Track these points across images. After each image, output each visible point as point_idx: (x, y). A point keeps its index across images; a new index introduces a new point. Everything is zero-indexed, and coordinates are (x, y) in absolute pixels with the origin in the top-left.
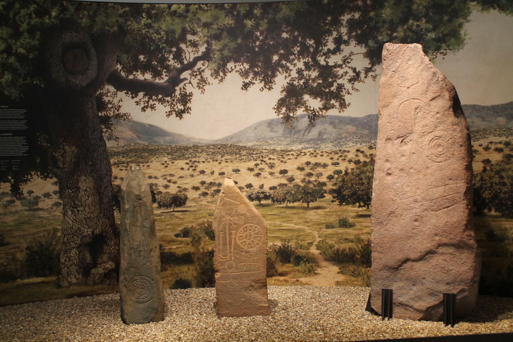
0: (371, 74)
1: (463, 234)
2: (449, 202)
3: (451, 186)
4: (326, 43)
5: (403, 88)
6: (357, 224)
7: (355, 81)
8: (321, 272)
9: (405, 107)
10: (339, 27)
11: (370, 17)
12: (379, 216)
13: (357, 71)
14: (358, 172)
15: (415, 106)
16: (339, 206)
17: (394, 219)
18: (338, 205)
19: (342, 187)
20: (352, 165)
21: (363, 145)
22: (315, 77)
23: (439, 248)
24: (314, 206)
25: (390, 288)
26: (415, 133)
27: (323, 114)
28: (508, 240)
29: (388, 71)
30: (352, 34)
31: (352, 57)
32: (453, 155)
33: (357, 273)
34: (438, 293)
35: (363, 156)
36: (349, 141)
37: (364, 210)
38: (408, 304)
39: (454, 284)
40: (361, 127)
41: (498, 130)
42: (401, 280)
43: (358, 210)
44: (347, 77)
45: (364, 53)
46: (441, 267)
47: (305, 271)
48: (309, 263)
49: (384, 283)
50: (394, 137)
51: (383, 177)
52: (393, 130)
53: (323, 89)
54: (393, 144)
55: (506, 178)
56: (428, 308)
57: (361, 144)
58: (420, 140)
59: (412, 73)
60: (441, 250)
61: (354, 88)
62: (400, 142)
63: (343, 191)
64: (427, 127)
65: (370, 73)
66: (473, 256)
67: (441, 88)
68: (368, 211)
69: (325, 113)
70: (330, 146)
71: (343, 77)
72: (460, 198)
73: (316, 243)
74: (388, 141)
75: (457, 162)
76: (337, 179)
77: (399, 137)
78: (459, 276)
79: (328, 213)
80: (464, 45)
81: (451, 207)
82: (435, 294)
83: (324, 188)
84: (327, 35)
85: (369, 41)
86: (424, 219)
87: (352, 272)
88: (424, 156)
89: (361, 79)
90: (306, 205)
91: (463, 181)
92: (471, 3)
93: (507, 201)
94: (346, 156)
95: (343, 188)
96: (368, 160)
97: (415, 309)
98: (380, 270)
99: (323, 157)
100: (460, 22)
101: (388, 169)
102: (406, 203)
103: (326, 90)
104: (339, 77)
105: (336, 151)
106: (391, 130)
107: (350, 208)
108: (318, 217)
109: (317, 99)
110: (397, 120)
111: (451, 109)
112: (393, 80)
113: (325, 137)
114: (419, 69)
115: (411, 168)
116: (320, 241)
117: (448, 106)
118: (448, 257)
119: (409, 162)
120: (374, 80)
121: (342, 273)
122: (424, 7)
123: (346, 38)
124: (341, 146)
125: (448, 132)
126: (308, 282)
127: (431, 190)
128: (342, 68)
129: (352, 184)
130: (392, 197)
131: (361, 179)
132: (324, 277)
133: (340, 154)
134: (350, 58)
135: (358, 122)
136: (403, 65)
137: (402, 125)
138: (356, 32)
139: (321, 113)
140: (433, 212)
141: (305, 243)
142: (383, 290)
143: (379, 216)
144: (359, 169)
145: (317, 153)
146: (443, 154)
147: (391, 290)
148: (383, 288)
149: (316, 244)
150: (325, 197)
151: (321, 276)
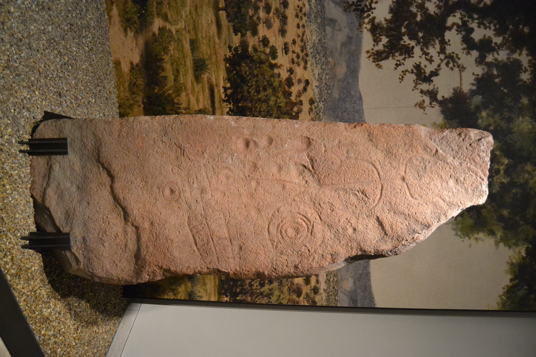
0: (427, 100)
1: (154, 264)
2: (204, 245)
3: (230, 248)
4: (484, 25)
5: (404, 169)
6: (200, 86)
7: (416, 75)
8: (129, 37)
9: (367, 172)
10: (508, 46)
11: (520, 98)
12: (177, 128)
13: (432, 78)
14: (276, 84)
15: (369, 190)
16: (224, 57)
17: (173, 155)
18: (225, 55)
19: (252, 61)
20: (284, 75)
21: (316, 91)
22: (427, 9)
23: (133, 228)
24: (221, 18)
25: (69, 150)
27: (365, 25)
28: (192, 286)
29: (437, 140)
30: (495, 69)
31: (456, 70)
33: (135, 89)
34: (69, 225)
35: (299, 90)
36: (321, 68)
37: (220, 95)
38: (51, 180)
39: (85, 248)
40: (343, 86)
41: (336, 279)
42: (83, 167)
43: (220, 87)
44: (424, 62)
45: (461, 89)
46: (107, 230)
47: (127, 13)
48: (139, 18)
49: (76, 140)
50: (313, 152)
52: (325, 151)
53: (406, 23)
55: (270, 287)
56: (48, 209)
57: (316, 86)
58: (306, 198)
60: (130, 230)
61: (405, 74)
62: (304, 163)
63: (246, 63)
64: (329, 210)
65: (428, 98)
66: (126, 277)
67: (399, 236)
68: (220, 102)
69: (366, 28)
70: (314, 38)
71: (424, 56)
72: (210, 263)
73: (168, 26)
75: (269, 260)
76: (264, 52)
77: (312, 161)
78: (96, 257)
79: (212, 43)
80: (461, 238)
81: (195, 248)
82: (68, 221)
83: (249, 34)
84: (497, 26)
85: (480, 97)
86: (174, 204)
87: (135, 83)
89: (420, 84)
90: (221, 6)
91: (238, 268)
92: (524, 249)
93: (241, 288)
94: (299, 65)
95: (250, 63)
96: (293, 98)
97: (45, 189)
98: (94, 134)
99: (295, 29)
100: (496, 232)
101: (256, 144)
102: (199, 175)
103: (405, 28)
104: (425, 49)
105: (306, 49)
106: (325, 146)
107: (222, 74)
108: (205, 25)
109: (389, 13)
110: (343, 158)
111: (360, 253)
112: (420, 151)
113: (328, 29)
114: (437, 198)
115: (258, 183)
116: (172, 33)
117: (367, 248)
118: (121, 240)
119: (268, 180)
120: (416, 105)
121: (132, 68)
122: (527, 182)
123: (490, 58)
124: (314, 57)
126: (112, 19)
127: (222, 215)
128: (439, 53)
129: (257, 76)
130: (208, 151)
131: (265, 89)
132: (123, 43)
133: (301, 55)
134: (454, 66)
135: (350, 81)
136: (448, 169)
137: (335, 167)
138: (498, 76)
139: (366, 20)
140: (186, 219)
141: (165, 9)
142: (66, 139)
143: (177, 128)
144: (280, 86)
145: (301, 18)
146: (283, 237)
147: (66, 153)
148: (69, 140)
149: (166, 27)
150: (236, 35)
151: (123, 37)
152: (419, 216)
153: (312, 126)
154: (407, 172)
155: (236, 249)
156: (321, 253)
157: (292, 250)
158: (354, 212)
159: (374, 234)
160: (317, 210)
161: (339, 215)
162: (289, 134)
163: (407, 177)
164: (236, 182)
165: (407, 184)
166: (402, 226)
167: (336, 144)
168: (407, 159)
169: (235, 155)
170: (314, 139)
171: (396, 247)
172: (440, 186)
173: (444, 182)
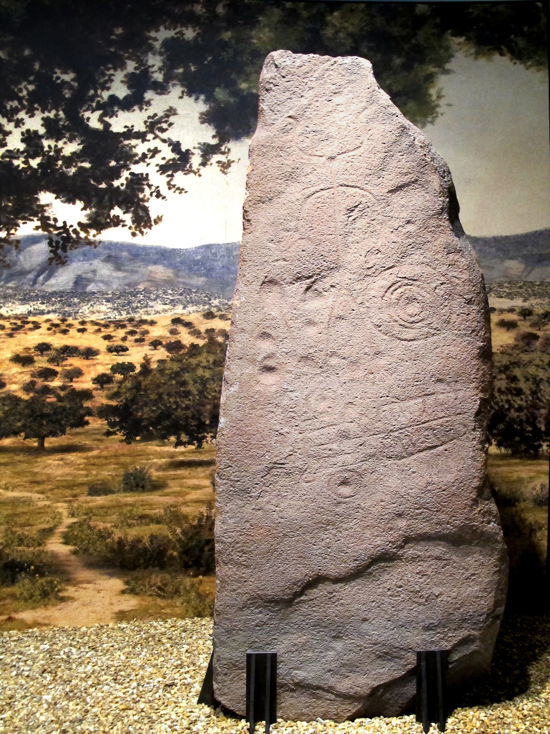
9: (319, 205)
50: (285, 276)
58: (359, 287)
67: (419, 165)
88: (370, 326)
110: (297, 236)
111: (445, 216)
117: (438, 207)
137: (310, 247)
152: (388, 139)
153: (244, 279)
158: (381, 223)
163: (329, 154)
166: (404, 161)
167: (274, 246)
170: (265, 275)
171: (436, 169)
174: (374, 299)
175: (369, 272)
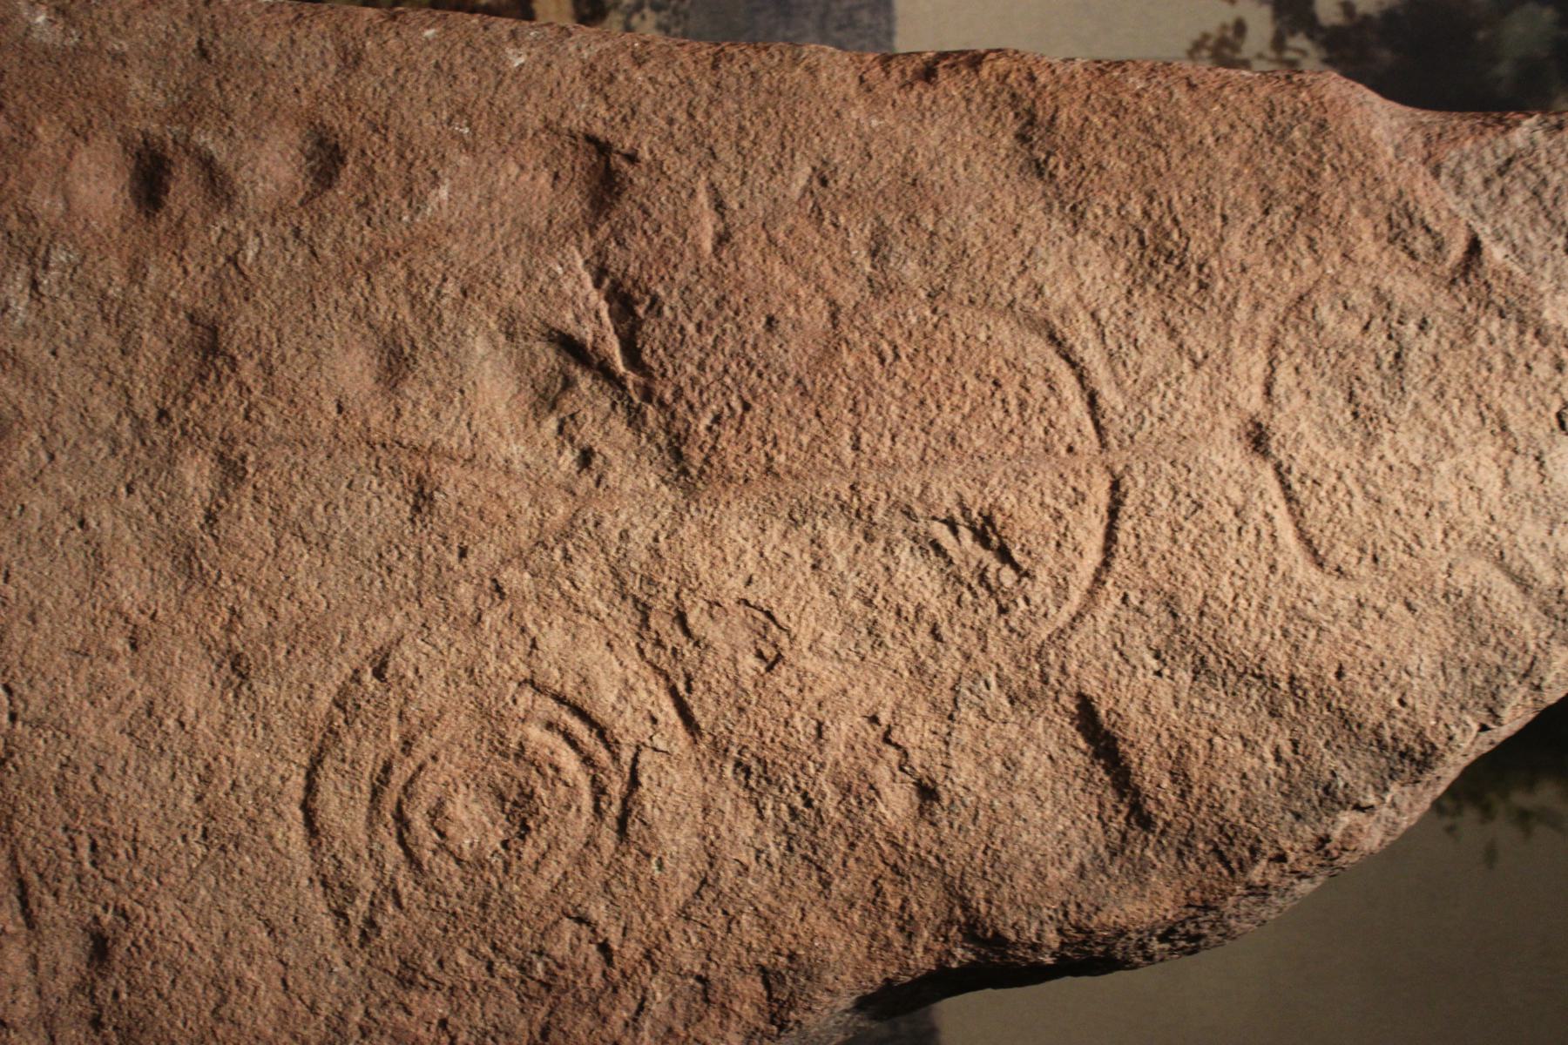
5: (1259, 371)
9: (1011, 390)
26: (678, 515)
29: (1475, 180)
32: (408, 976)
50: (638, 243)
51: (116, 100)
52: (722, 239)
54: (538, 240)
58: (584, 574)
59: (1444, 489)
64: (749, 662)
65: (1266, 11)
74: (576, 163)
85: (1548, 14)
88: (381, 629)
106: (719, 206)
110: (848, 293)
111: (961, 954)
112: (1368, 247)
114: (1481, 568)
115: (231, 470)
117: (1009, 921)
119: (306, 442)
120: (1197, 46)
125: (684, 914)
136: (1543, 369)
137: (792, 355)
152: (1363, 688)
153: (624, 60)
154: (1278, 390)
155: (67, 960)
156: (690, 962)
157: (485, 949)
158: (921, 669)
159: (1063, 822)
160: (664, 661)
161: (820, 693)
162: (462, 111)
163: (1281, 426)
164: (62, 459)
165: (1281, 473)
166: (1250, 762)
167: (796, 190)
168: (1282, 300)
169: (59, 256)
170: (645, 155)
171: (1206, 907)
172: (1494, 488)
173: (1518, 460)
174: (522, 647)
175: (660, 622)
